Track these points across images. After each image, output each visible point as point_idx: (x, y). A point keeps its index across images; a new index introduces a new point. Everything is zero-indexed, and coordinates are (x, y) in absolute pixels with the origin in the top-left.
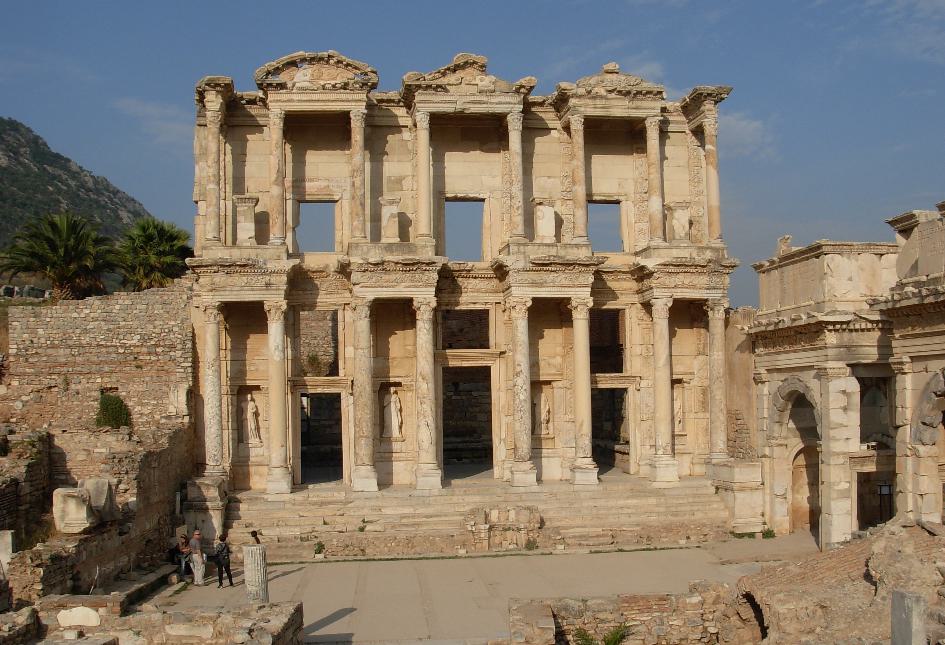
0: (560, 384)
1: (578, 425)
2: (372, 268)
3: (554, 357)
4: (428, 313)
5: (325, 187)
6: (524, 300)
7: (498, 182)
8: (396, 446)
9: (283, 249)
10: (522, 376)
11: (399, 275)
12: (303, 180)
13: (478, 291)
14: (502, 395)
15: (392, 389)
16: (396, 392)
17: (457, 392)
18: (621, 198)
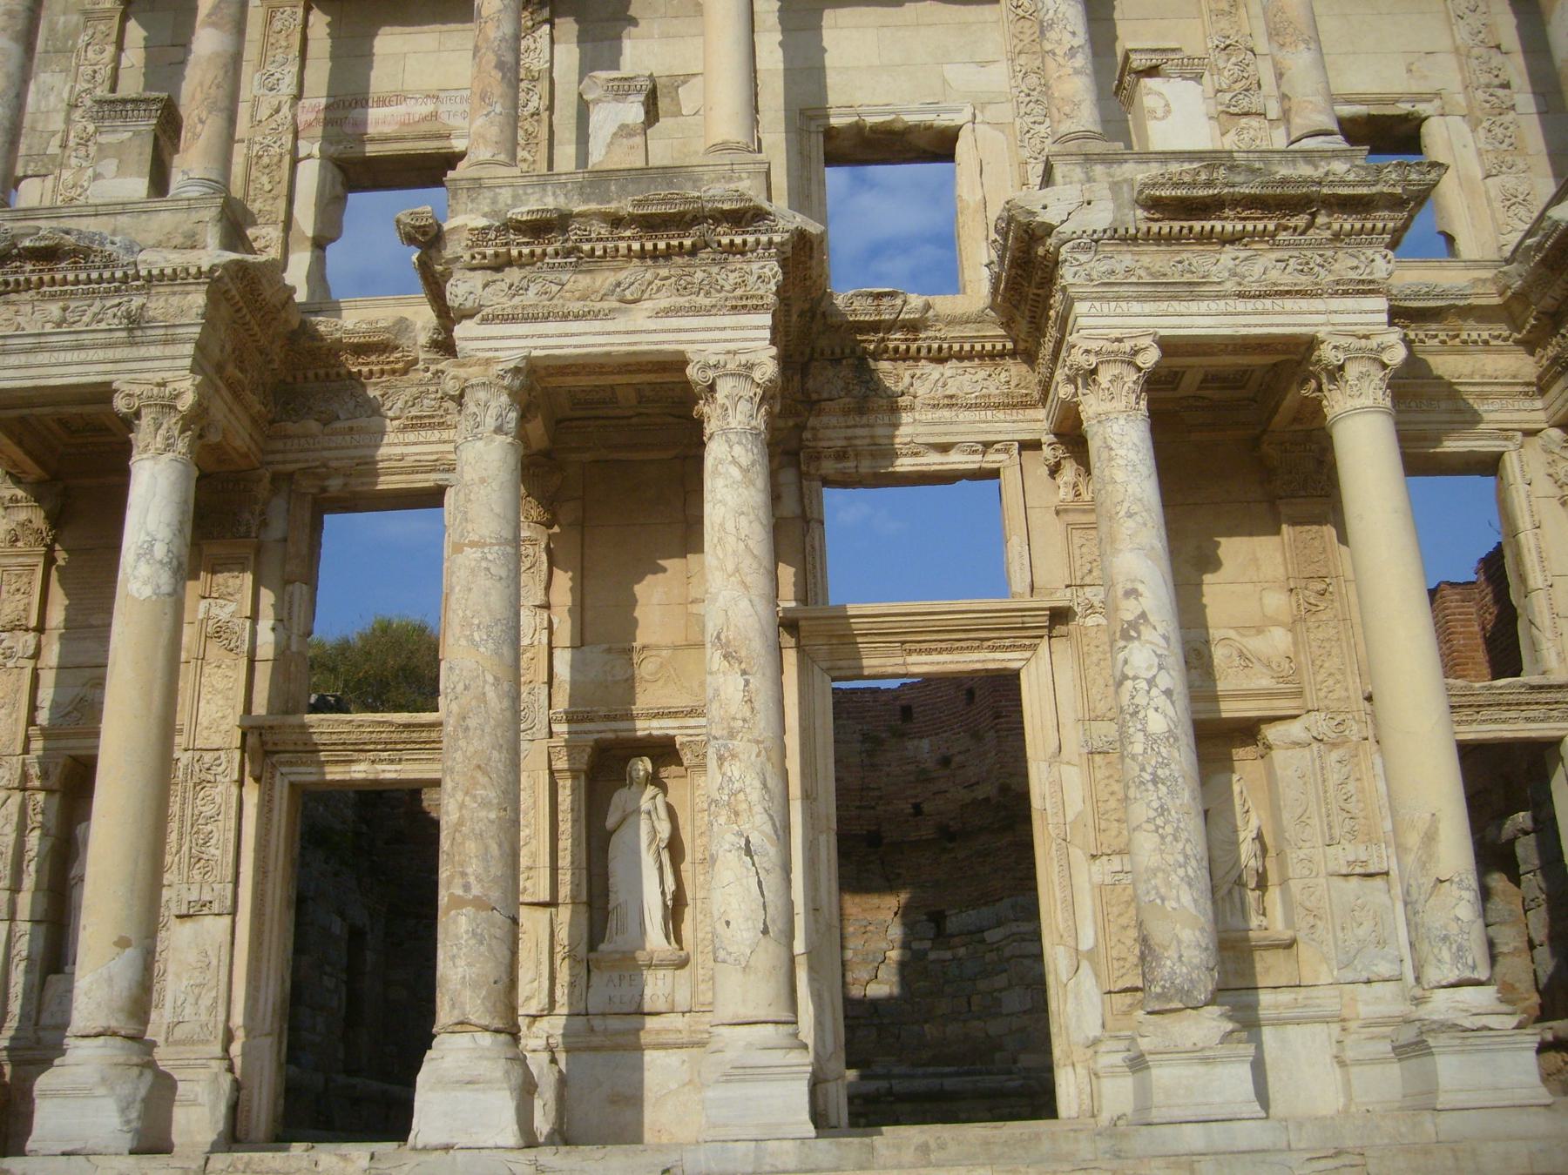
0: (1295, 729)
1: (1413, 839)
2: (520, 247)
3: (1260, 630)
4: (744, 407)
5: (424, 119)
6: (1127, 346)
7: (998, 78)
8: (656, 988)
9: (210, 213)
10: (1147, 633)
11: (632, 273)
12: (362, 101)
13: (951, 402)
14: (1073, 778)
15: (644, 765)
16: (655, 779)
17: (941, 936)
18: (1422, 108)
